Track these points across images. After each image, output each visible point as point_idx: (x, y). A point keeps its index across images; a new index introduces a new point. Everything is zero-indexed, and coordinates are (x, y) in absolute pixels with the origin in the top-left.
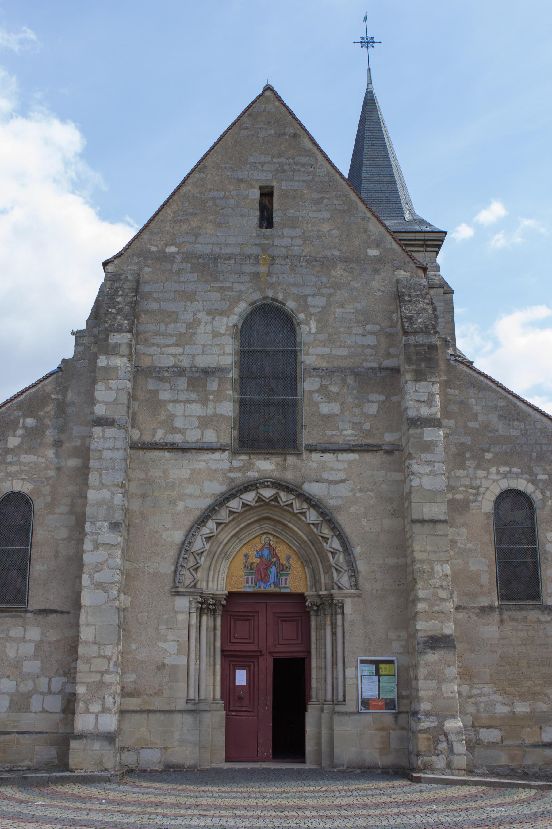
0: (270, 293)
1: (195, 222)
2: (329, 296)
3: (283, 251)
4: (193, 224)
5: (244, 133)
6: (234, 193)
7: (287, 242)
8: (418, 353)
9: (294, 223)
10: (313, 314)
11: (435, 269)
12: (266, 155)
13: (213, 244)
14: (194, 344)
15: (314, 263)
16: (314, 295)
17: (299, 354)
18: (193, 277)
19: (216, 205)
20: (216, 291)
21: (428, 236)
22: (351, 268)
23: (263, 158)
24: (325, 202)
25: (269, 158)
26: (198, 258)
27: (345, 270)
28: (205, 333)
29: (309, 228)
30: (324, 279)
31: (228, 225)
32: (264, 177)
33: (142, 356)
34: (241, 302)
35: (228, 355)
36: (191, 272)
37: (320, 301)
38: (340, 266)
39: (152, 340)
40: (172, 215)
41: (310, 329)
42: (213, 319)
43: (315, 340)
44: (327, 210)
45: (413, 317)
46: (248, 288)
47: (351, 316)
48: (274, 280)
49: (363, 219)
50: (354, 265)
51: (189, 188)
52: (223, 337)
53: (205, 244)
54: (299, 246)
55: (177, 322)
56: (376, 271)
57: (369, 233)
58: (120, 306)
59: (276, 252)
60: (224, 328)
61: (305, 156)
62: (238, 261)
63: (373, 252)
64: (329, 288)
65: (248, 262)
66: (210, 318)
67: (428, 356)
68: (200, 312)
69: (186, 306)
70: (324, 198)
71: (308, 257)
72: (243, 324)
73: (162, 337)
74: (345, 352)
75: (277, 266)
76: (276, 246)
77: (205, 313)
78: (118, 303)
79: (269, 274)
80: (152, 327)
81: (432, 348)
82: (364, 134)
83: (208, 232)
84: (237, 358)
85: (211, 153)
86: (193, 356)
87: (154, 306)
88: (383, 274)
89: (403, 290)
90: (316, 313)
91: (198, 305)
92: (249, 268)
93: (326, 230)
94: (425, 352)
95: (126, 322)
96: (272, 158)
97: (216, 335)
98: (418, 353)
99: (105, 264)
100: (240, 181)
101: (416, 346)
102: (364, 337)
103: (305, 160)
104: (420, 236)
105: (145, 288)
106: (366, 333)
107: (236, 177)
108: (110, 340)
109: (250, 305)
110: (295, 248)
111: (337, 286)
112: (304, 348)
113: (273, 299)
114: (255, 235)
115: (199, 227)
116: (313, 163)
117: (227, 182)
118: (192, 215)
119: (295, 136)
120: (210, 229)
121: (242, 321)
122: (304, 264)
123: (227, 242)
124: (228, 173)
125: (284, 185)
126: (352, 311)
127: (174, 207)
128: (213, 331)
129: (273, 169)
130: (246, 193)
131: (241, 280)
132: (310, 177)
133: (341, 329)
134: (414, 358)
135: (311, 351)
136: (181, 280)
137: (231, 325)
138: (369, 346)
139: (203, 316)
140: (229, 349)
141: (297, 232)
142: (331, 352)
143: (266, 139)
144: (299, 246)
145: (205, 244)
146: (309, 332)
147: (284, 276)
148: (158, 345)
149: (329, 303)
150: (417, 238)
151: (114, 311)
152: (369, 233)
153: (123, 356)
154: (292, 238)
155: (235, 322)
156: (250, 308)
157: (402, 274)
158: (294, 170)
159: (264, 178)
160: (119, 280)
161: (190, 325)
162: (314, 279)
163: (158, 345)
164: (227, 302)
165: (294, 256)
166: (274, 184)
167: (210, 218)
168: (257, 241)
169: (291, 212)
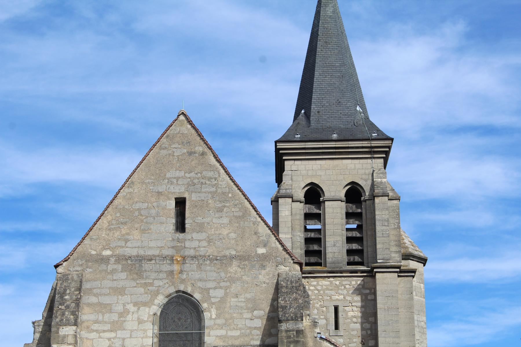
0: (182, 288)
1: (124, 230)
2: (226, 288)
3: (192, 253)
4: (124, 232)
5: (164, 152)
6: (155, 204)
7: (195, 244)
8: (289, 337)
9: (201, 228)
10: (213, 304)
11: (381, 175)
12: (180, 171)
13: (138, 247)
14: (124, 329)
15: (215, 262)
16: (215, 288)
17: (203, 335)
18: (123, 275)
19: (141, 215)
20: (141, 287)
21: (375, 143)
22: (244, 265)
23: (178, 174)
24: (225, 209)
25: (182, 174)
26: (126, 260)
27: (239, 266)
28: (132, 320)
29: (213, 232)
30: (223, 275)
31: (150, 231)
32: (179, 191)
33: (85, 340)
34: (159, 295)
35: (150, 337)
36: (122, 272)
37: (220, 293)
38: (235, 263)
39: (92, 327)
40: (108, 224)
41: (211, 315)
42: (139, 309)
43: (215, 324)
44: (227, 217)
45: (287, 307)
46: (165, 284)
47: (243, 304)
48: (184, 276)
49: (254, 224)
50: (246, 262)
51: (120, 201)
52: (146, 323)
53: (132, 248)
54: (204, 247)
55: (111, 312)
56: (263, 267)
57: (259, 235)
58: (68, 303)
59: (188, 253)
60: (147, 316)
61: (211, 171)
62: (157, 261)
63: (261, 251)
64: (226, 282)
65: (165, 262)
66: (135, 309)
67: (296, 339)
68: (128, 304)
69: (118, 299)
70: (225, 206)
71: (211, 257)
72: (162, 311)
73: (100, 325)
74: (237, 333)
75: (187, 265)
76: (187, 248)
77: (132, 304)
78: (66, 300)
79: (181, 272)
80: (92, 317)
81: (299, 332)
82: (318, 30)
83: (135, 237)
84: (156, 340)
85: (137, 170)
86: (124, 339)
87: (93, 300)
88: (268, 269)
89: (282, 283)
90: (216, 302)
91: (127, 298)
92: (166, 267)
93: (225, 233)
94: (294, 336)
95: (72, 317)
96: (185, 173)
97: (140, 322)
98: (289, 337)
99: (56, 266)
100: (159, 193)
101: (287, 331)
102: (252, 321)
103: (210, 174)
104: (365, 144)
105: (86, 286)
106: (253, 318)
107: (157, 191)
108: (60, 333)
109: (167, 297)
110: (202, 249)
111: (232, 280)
112: (206, 331)
113: (184, 292)
114: (171, 239)
115: (128, 234)
116: (217, 176)
117: (149, 195)
118: (122, 223)
119: (203, 154)
120: (136, 235)
121: (160, 310)
122: (208, 262)
123: (150, 246)
124: (151, 188)
125: (194, 197)
126: (243, 300)
127: (109, 217)
128: (138, 319)
129: (185, 183)
130: (164, 204)
131: (160, 277)
132: (214, 189)
133: (235, 315)
134: (285, 341)
135: (212, 333)
136: (114, 278)
137: (152, 313)
138: (255, 328)
139: (131, 308)
140: (150, 333)
141: (203, 236)
142: (227, 333)
143: (180, 157)
144: (204, 247)
145: (132, 248)
146: (211, 318)
147: (193, 273)
148: (97, 331)
149: (226, 294)
150: (364, 145)
151: (63, 307)
152: (259, 235)
153: (70, 344)
154: (200, 241)
155: (154, 311)
156: (167, 300)
157: (283, 269)
158: (202, 183)
159: (178, 191)
160: (67, 279)
161: (121, 315)
162: (215, 274)
163: (97, 331)
164: (149, 295)
165: (200, 256)
166: (186, 195)
167: (137, 226)
168: (172, 244)
169: (199, 219)
